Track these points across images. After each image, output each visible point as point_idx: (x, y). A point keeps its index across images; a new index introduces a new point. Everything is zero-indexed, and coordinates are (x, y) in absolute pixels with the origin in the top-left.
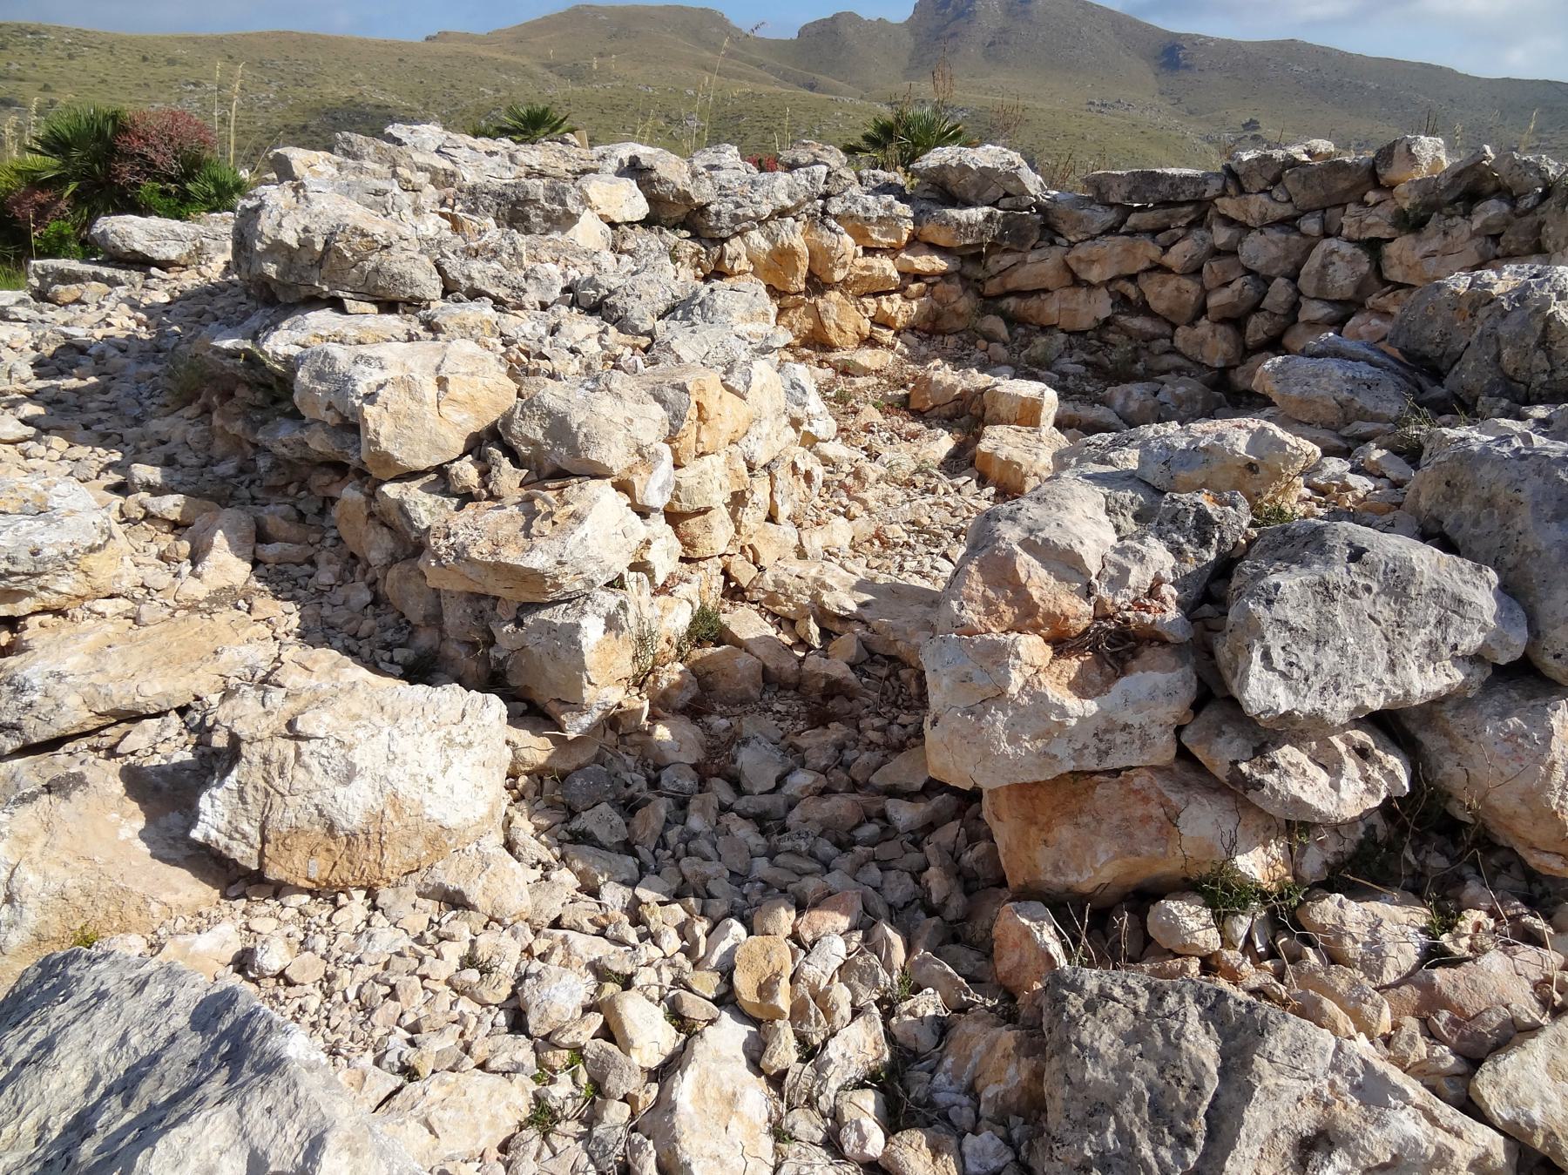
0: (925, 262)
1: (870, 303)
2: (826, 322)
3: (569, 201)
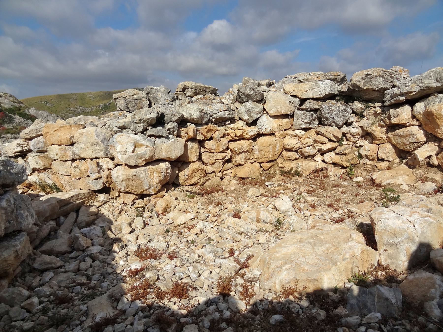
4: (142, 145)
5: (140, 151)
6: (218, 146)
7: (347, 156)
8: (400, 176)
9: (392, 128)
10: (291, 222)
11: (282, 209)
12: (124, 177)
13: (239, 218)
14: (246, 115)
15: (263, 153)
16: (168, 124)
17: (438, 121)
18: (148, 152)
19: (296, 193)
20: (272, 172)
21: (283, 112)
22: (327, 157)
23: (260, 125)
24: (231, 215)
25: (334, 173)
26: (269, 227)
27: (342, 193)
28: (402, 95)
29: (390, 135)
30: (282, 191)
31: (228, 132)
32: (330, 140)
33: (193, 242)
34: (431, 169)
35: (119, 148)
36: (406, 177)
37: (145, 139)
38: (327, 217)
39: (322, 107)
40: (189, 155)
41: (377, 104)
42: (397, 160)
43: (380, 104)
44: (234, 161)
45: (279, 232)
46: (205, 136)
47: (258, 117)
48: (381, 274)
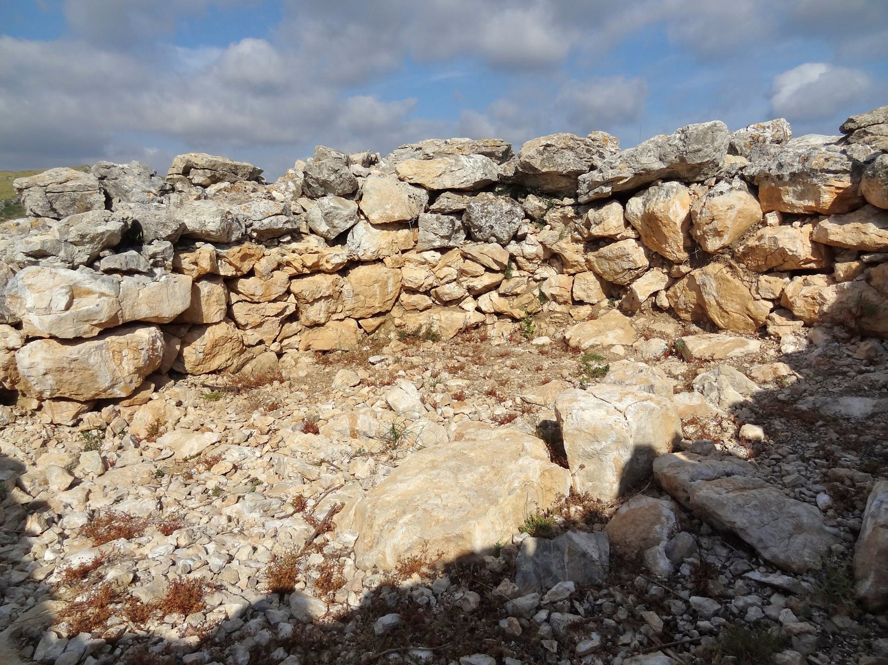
0: (839, 232)
1: (773, 284)
2: (706, 297)
4: (89, 292)
5: (84, 305)
6: (268, 288)
7: (520, 298)
8: (610, 331)
9: (594, 243)
10: (417, 431)
11: (401, 407)
12: (49, 365)
13: (316, 432)
14: (324, 223)
15: (362, 298)
16: (150, 244)
17: (664, 230)
18: (106, 307)
19: (428, 373)
20: (382, 336)
21: (397, 216)
22: (484, 302)
23: (353, 244)
24: (298, 427)
25: (499, 332)
26: (376, 446)
27: (513, 367)
28: (606, 183)
29: (591, 256)
30: (401, 373)
31: (286, 258)
32: (489, 269)
33: (218, 491)
34: (658, 315)
35: (30, 299)
36: (620, 332)
37: (96, 279)
38: (484, 416)
39: (470, 207)
40: (204, 309)
41: (568, 201)
42: (605, 302)
43: (571, 201)
44: (303, 318)
45: (394, 453)
46: (238, 269)
47: (348, 226)
48: (575, 510)
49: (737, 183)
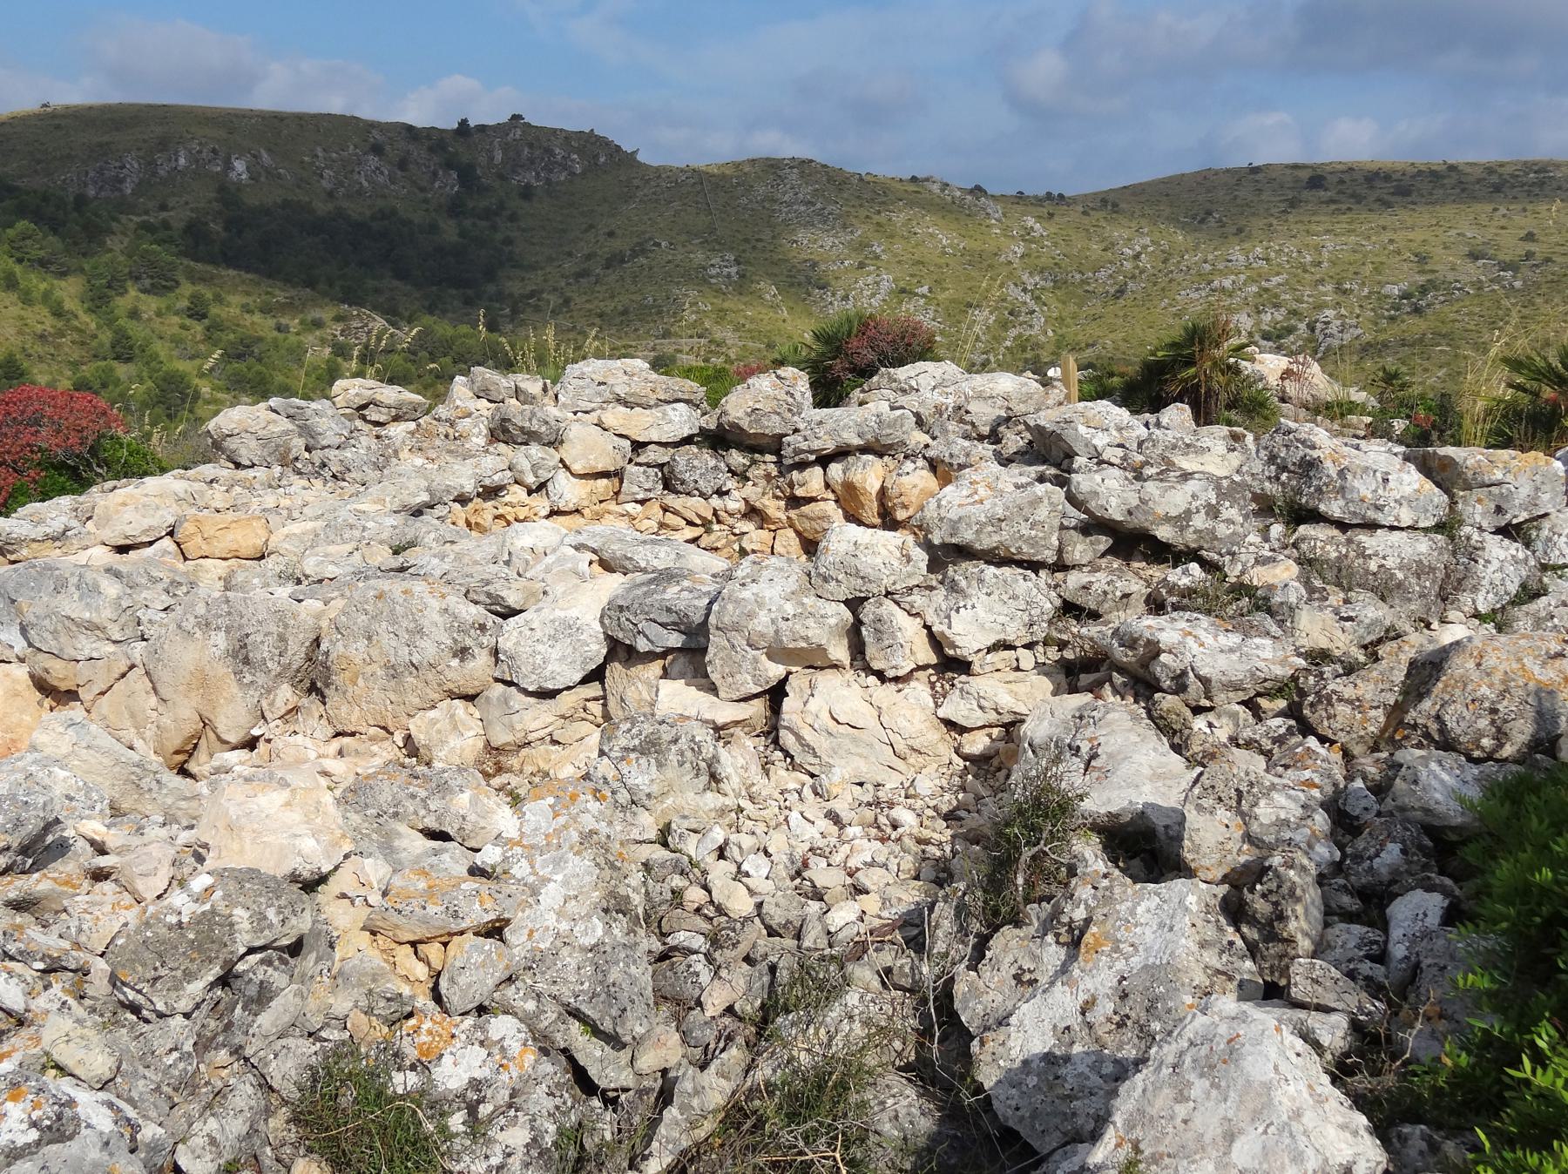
3: (534, 421)
9: (794, 502)
21: (600, 467)
28: (811, 452)
29: (793, 514)
41: (769, 458)
43: (774, 458)
49: (921, 462)
